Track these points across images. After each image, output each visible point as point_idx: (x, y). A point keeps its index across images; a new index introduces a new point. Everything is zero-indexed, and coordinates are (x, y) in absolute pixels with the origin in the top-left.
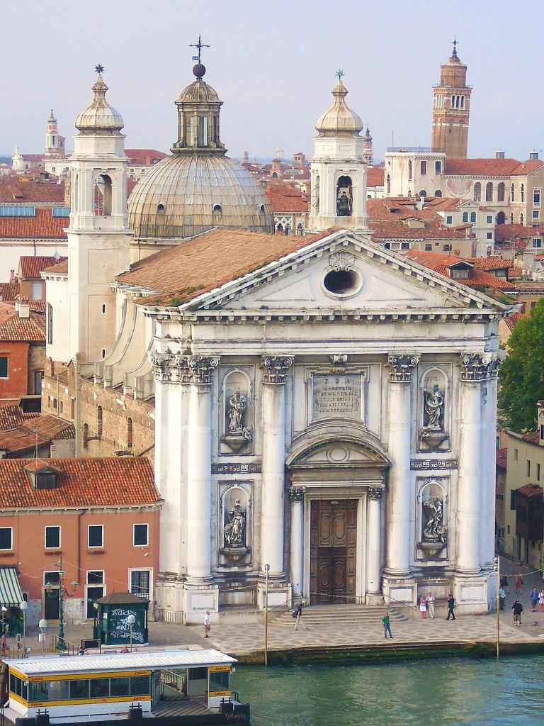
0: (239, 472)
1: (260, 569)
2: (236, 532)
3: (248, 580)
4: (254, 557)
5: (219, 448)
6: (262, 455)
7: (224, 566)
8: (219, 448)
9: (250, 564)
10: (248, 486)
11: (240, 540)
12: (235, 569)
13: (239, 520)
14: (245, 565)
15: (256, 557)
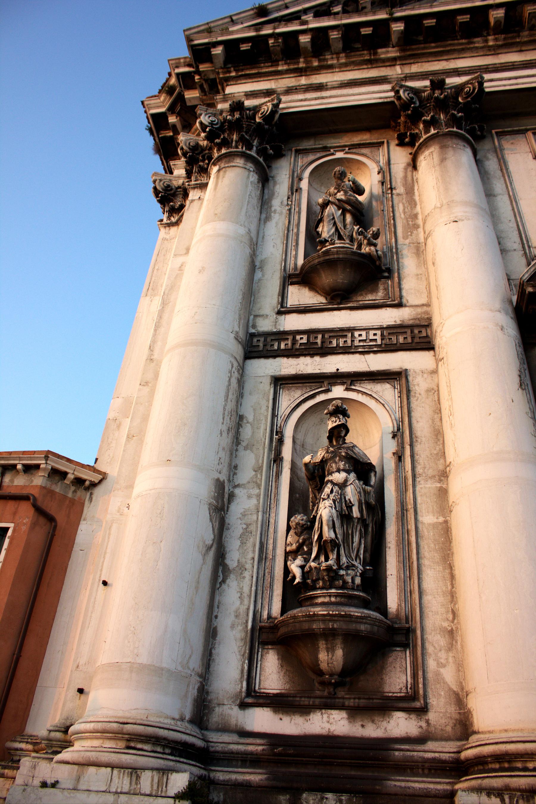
0: (346, 351)
1: (464, 728)
2: (328, 534)
3: (399, 783)
4: (431, 664)
5: (283, 294)
6: (428, 305)
7: (279, 703)
8: (283, 294)
9: (413, 702)
10: (386, 391)
11: (353, 577)
12: (331, 723)
13: (343, 485)
14: (385, 706)
15: (439, 666)
